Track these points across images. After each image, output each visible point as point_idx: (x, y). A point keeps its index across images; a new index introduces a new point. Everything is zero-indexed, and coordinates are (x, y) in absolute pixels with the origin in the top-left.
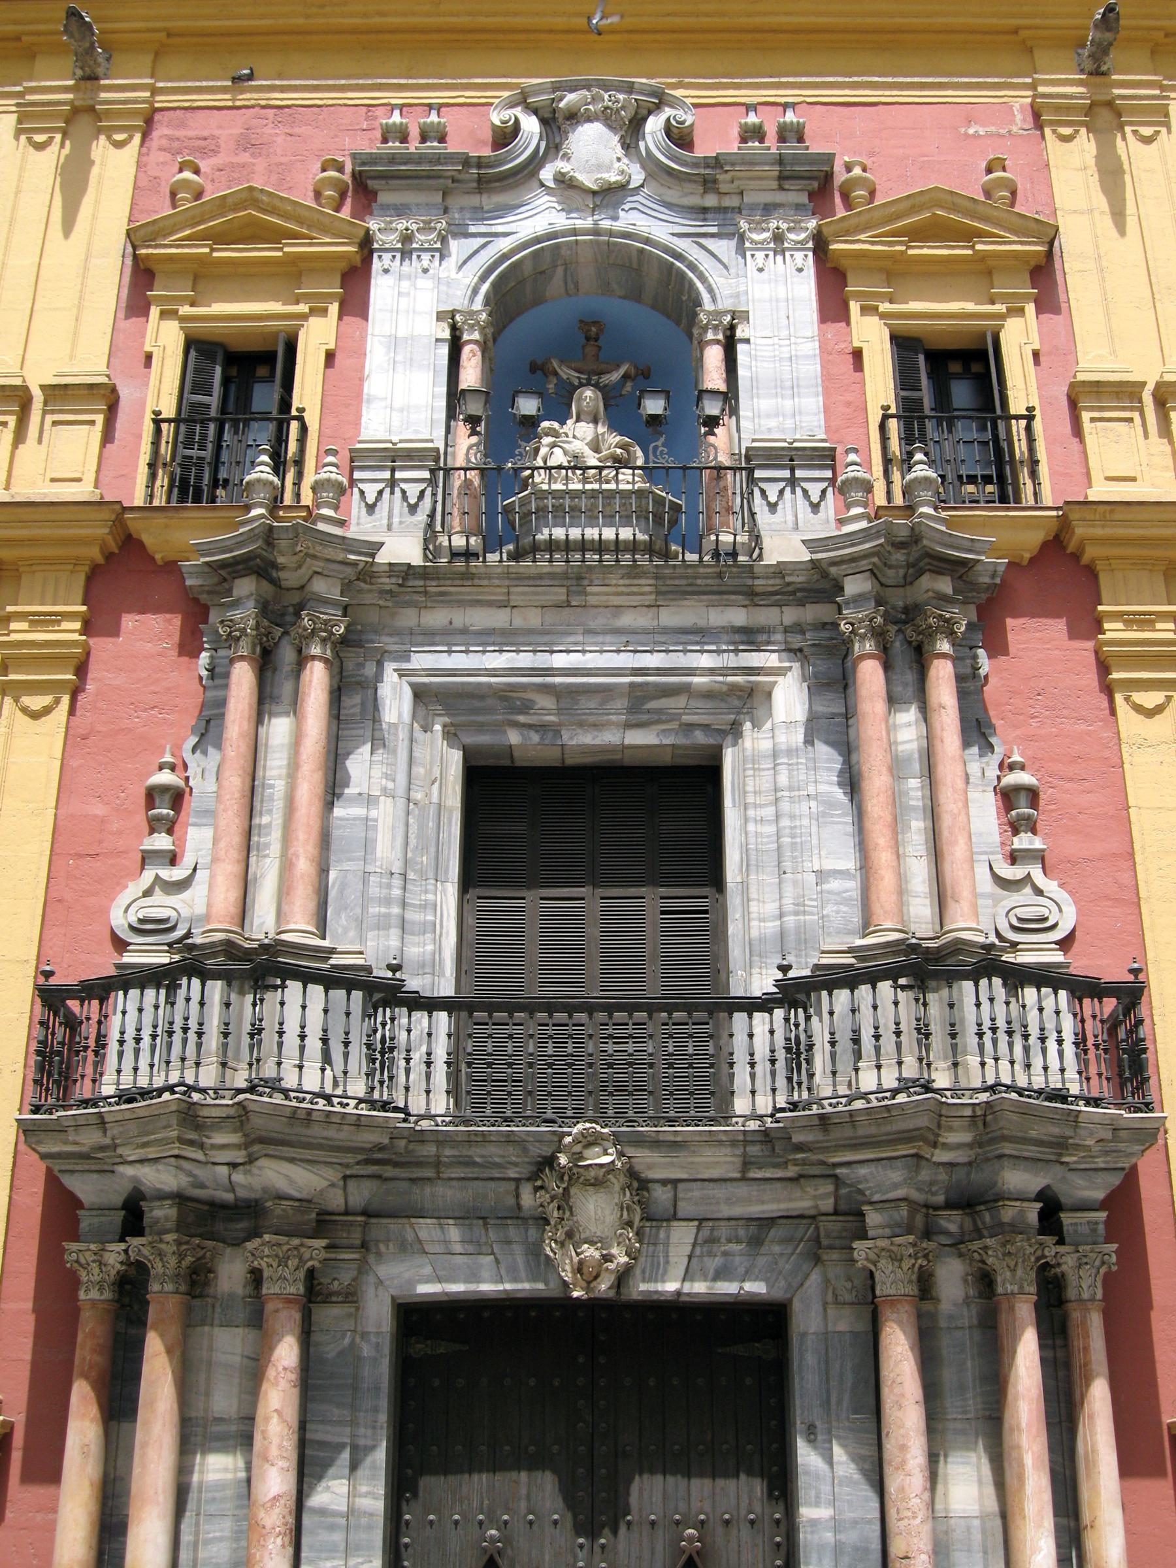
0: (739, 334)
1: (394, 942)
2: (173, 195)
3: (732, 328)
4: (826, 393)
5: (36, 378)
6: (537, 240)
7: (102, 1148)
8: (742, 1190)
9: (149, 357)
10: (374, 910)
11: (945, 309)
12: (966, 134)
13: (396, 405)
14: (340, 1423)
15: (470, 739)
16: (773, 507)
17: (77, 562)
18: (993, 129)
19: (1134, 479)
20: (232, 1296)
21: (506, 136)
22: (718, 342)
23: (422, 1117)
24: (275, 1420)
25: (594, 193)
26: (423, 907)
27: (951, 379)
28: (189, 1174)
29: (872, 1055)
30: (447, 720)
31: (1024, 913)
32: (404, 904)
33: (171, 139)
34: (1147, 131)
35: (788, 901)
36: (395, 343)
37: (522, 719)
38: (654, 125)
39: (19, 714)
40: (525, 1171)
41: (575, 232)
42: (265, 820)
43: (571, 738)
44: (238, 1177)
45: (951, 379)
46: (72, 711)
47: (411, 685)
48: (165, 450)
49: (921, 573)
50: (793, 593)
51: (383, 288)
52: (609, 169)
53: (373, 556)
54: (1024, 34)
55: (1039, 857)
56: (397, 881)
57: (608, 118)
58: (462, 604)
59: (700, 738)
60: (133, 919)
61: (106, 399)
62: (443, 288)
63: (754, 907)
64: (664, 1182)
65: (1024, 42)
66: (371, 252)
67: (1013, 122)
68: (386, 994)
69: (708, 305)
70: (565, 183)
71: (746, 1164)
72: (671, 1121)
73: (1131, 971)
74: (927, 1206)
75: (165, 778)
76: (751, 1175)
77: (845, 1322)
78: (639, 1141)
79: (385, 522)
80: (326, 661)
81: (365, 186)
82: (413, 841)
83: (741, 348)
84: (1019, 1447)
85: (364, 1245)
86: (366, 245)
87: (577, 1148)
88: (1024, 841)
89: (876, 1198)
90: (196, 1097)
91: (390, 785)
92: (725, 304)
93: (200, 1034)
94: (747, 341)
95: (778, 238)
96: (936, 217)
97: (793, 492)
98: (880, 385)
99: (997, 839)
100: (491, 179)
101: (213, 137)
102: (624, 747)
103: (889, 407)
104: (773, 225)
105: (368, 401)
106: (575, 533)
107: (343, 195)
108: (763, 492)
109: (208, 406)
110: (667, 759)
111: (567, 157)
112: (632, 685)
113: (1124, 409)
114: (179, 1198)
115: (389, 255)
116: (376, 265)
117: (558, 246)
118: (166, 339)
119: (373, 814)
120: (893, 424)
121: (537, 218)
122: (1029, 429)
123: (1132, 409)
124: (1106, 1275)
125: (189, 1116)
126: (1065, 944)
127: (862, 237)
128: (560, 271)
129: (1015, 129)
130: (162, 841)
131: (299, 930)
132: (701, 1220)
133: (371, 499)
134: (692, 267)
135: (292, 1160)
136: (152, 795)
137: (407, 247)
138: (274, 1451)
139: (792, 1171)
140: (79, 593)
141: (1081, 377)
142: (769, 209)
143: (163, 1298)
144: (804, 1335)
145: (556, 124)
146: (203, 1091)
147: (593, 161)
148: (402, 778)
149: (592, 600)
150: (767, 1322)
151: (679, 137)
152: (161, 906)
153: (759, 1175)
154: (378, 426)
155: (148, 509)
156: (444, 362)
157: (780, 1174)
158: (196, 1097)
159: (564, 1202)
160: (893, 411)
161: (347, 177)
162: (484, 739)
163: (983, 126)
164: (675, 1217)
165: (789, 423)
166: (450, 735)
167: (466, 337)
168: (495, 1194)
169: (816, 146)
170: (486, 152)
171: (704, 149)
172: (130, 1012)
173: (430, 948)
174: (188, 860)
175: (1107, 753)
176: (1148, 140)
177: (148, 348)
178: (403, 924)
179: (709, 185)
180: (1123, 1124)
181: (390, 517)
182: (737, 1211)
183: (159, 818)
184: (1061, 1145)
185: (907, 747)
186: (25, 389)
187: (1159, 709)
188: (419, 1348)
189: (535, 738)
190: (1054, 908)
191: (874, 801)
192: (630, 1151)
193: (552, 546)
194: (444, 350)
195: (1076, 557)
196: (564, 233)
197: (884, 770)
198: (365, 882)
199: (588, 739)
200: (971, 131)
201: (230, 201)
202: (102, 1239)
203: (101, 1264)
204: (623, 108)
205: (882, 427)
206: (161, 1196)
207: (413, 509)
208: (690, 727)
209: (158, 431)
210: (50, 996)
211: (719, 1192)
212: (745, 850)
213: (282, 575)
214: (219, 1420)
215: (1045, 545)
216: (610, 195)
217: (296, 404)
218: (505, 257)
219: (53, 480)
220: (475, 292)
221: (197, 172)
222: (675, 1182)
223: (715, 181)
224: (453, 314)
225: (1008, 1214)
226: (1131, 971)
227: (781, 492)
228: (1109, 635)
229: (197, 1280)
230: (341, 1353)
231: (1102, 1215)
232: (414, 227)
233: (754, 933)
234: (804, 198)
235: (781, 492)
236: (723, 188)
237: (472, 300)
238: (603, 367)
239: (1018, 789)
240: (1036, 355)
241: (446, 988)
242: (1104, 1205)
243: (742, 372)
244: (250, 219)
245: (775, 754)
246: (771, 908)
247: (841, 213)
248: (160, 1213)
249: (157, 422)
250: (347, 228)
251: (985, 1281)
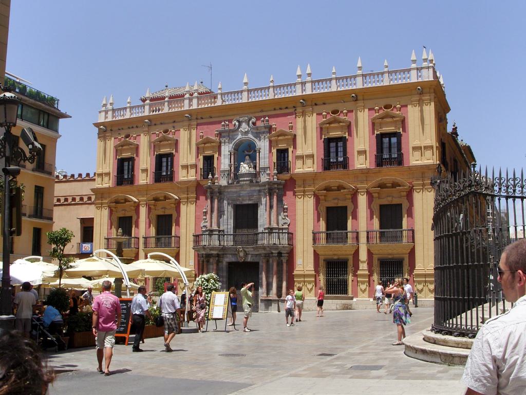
5: (189, 164)
21: (235, 125)
38: (251, 122)
51: (223, 148)
57: (245, 121)
61: (195, 166)
75: (205, 210)
81: (220, 134)
86: (220, 143)
88: (286, 214)
95: (265, 137)
98: (275, 159)
114: (205, 254)
118: (201, 158)
121: (240, 136)
130: (205, 217)
136: (204, 212)
141: (296, 155)
142: (264, 133)
151: (254, 124)
152: (205, 224)
162: (235, 203)
168: (234, 252)
179: (257, 129)
207: (227, 177)
216: (246, 133)
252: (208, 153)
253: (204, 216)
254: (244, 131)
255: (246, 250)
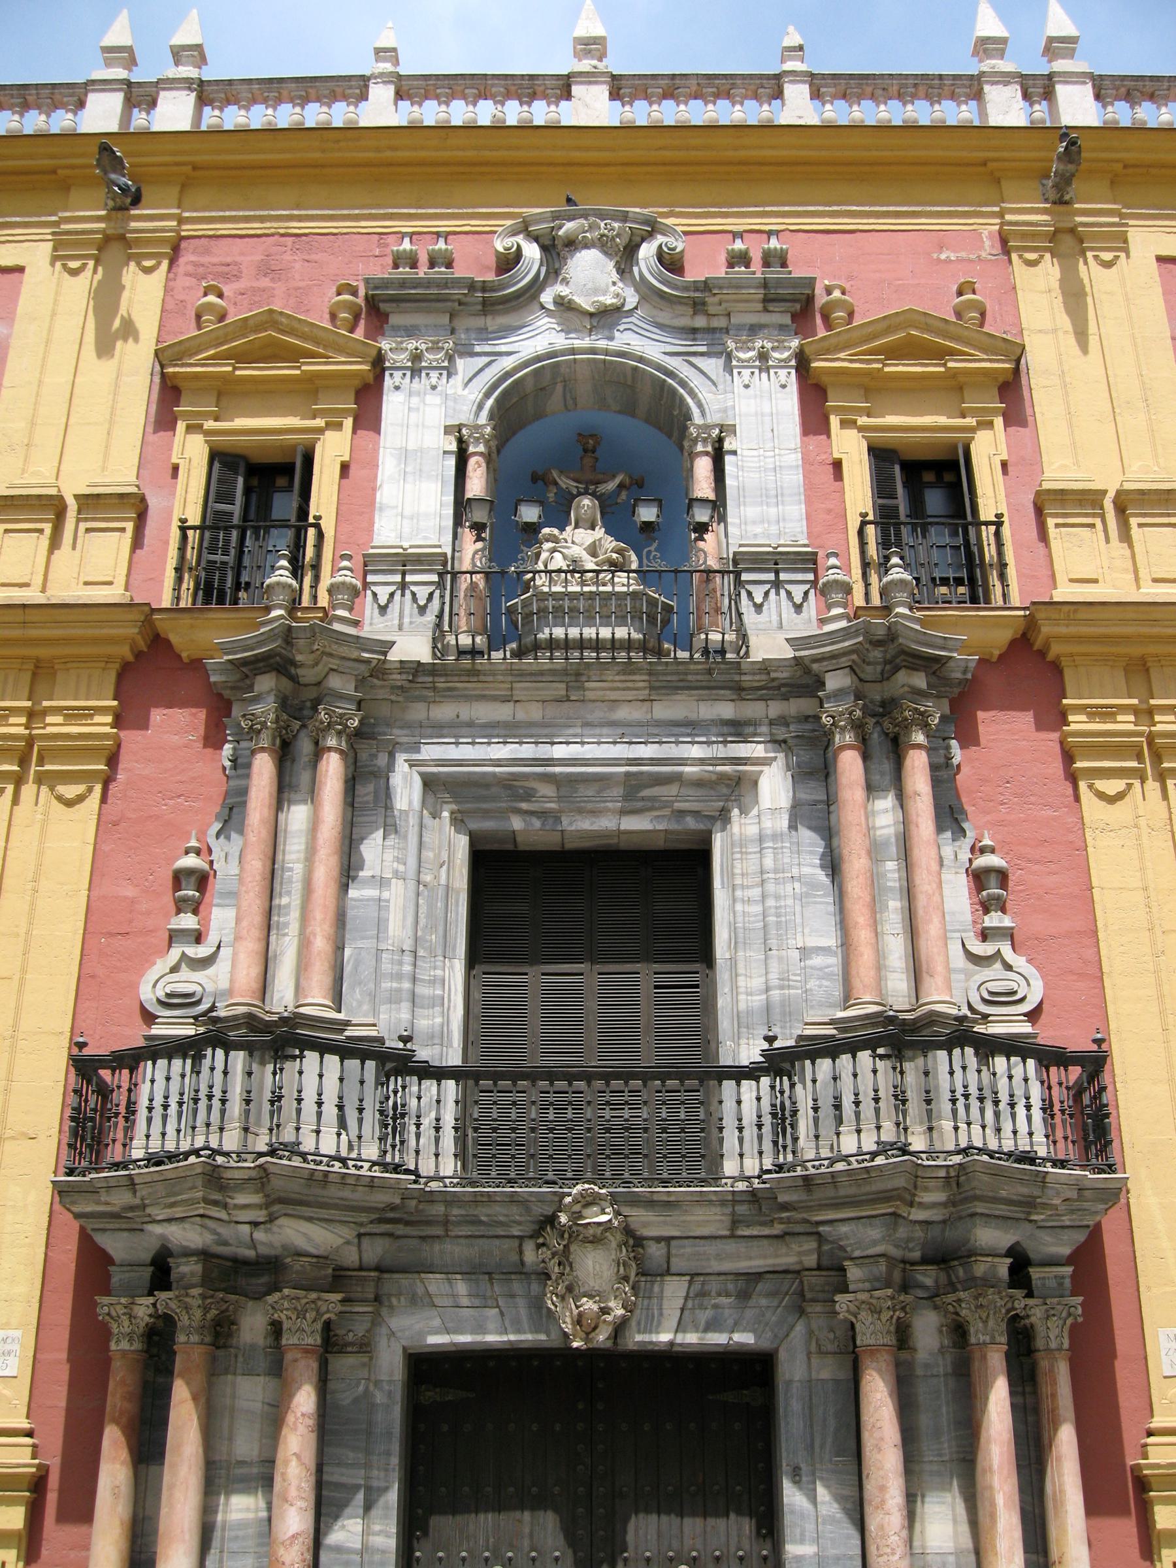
0: (727, 446)
1: (405, 1015)
2: (198, 317)
3: (720, 440)
4: (809, 502)
5: (71, 489)
6: (539, 359)
7: (132, 1208)
8: (731, 1246)
9: (176, 468)
10: (387, 985)
11: (919, 423)
12: (939, 260)
13: (407, 512)
14: (354, 1465)
15: (475, 825)
16: (759, 608)
17: (108, 660)
18: (963, 254)
19: (1096, 581)
20: (253, 1347)
21: (509, 262)
22: (707, 453)
23: (431, 1179)
24: (294, 1463)
25: (591, 315)
26: (432, 982)
27: (925, 488)
28: (214, 1232)
29: (853, 1120)
30: (454, 807)
31: (995, 987)
32: (414, 980)
33: (196, 265)
34: (1107, 256)
35: (774, 976)
36: (405, 455)
37: (524, 806)
38: (647, 251)
39: (54, 802)
40: (528, 1229)
41: (573, 351)
42: (284, 901)
43: (571, 824)
44: (259, 1235)
45: (925, 488)
46: (104, 799)
47: (421, 774)
48: (191, 555)
49: (897, 669)
50: (778, 688)
51: (393, 404)
52: (605, 293)
53: (385, 654)
54: (991, 165)
55: (1008, 934)
56: (408, 958)
57: (603, 244)
58: (469, 698)
59: (691, 823)
60: (160, 994)
61: (135, 507)
62: (450, 403)
63: (741, 981)
64: (659, 1240)
65: (992, 173)
66: (383, 370)
67: (982, 248)
68: (397, 1064)
69: (697, 419)
70: (564, 306)
71: (735, 1223)
72: (665, 1182)
73: (1095, 1041)
74: (904, 1261)
75: (191, 861)
76: (740, 1232)
77: (828, 1370)
78: (635, 1201)
79: (396, 622)
80: (341, 752)
81: (377, 309)
82: (422, 921)
83: (728, 459)
84: (991, 1488)
85: (377, 1299)
86: (379, 364)
87: (577, 1208)
88: (994, 920)
89: (857, 1254)
90: (220, 1160)
91: (401, 868)
92: (713, 418)
93: (223, 1101)
94: (734, 453)
95: (763, 356)
96: (911, 338)
97: (778, 594)
98: (858, 493)
99: (969, 917)
100: (495, 302)
101: (236, 263)
102: (620, 833)
103: (867, 514)
104: (759, 344)
105: (381, 509)
106: (574, 632)
107: (357, 317)
108: (749, 594)
109: (231, 514)
110: (660, 844)
111: (566, 282)
112: (627, 774)
113: (1086, 515)
114: (204, 1255)
115: (400, 373)
116: (388, 382)
117: (557, 364)
118: (191, 452)
119: (385, 895)
120: (871, 530)
121: (538, 338)
122: (997, 534)
123: (1094, 515)
124: (1074, 1326)
125: (214, 1178)
126: (1033, 1016)
127: (842, 355)
128: (559, 388)
129: (984, 255)
130: (188, 921)
131: (317, 1004)
132: (693, 1275)
133: (383, 600)
134: (683, 384)
135: (310, 1219)
136: (179, 877)
137: (417, 366)
138: (293, 1493)
139: (777, 1229)
140: (110, 689)
141: (1046, 486)
142: (754, 330)
143: (189, 1347)
144: (790, 1382)
145: (556, 251)
146: (227, 1154)
147: (590, 285)
148: (412, 861)
149: (590, 695)
150: (754, 1371)
151: (671, 263)
152: (188, 981)
153: (747, 1232)
154: (388, 533)
155: (175, 610)
156: (452, 472)
157: (766, 1231)
158: (220, 1160)
159: (565, 1260)
160: (871, 517)
161: (360, 301)
162: (488, 825)
163: (954, 251)
164: (668, 1272)
165: (774, 529)
166: (458, 821)
167: (471, 449)
168: (500, 1251)
169: (798, 271)
170: (491, 277)
171: (694, 274)
172: (158, 1081)
173: (438, 1020)
174: (212, 938)
175: (1071, 837)
176: (1108, 265)
177: (174, 460)
178: (413, 998)
179: (698, 306)
180: (1088, 1184)
181: (401, 617)
182: (727, 1266)
183: (185, 900)
184: (1029, 1204)
185: (885, 831)
186: (60, 498)
187: (1120, 796)
188: (430, 1395)
189: (537, 823)
190: (1023, 983)
191: (854, 882)
192: (626, 1211)
193: (552, 644)
194: (451, 462)
195: (1042, 654)
196: (563, 353)
197: (863, 853)
198: (378, 959)
199: (586, 824)
200: (943, 256)
201: (251, 323)
202: (131, 1292)
203: (131, 1317)
204: (618, 235)
205: (861, 532)
206: (187, 1253)
207: (422, 610)
208: (682, 813)
209: (184, 538)
210: (84, 1067)
211: (710, 1248)
212: (733, 928)
213: (300, 672)
214: (242, 1463)
215: (1013, 643)
216: (606, 317)
217: (313, 512)
218: (508, 375)
219: (86, 583)
220: (480, 407)
221: (220, 295)
222: (668, 1240)
223: (704, 304)
224: (459, 428)
225: (980, 1268)
226: (1095, 1041)
227: (767, 594)
228: (1073, 727)
229: (221, 1332)
230: (356, 1400)
231: (1069, 1270)
232: (424, 347)
233: (742, 1006)
234: (787, 320)
235: (767, 594)
236: (712, 310)
237: (477, 414)
238: (601, 476)
239: (988, 870)
240: (1004, 465)
241: (454, 1058)
242: (1069, 1260)
243: (729, 482)
244: (270, 339)
245: (761, 839)
246: (757, 982)
247: (822, 333)
248: (187, 1269)
249: (183, 529)
250: (360, 348)
251: (959, 1332)
252: (261, 425)
253: (181, 906)
254: (589, 304)
255: (648, 1223)
